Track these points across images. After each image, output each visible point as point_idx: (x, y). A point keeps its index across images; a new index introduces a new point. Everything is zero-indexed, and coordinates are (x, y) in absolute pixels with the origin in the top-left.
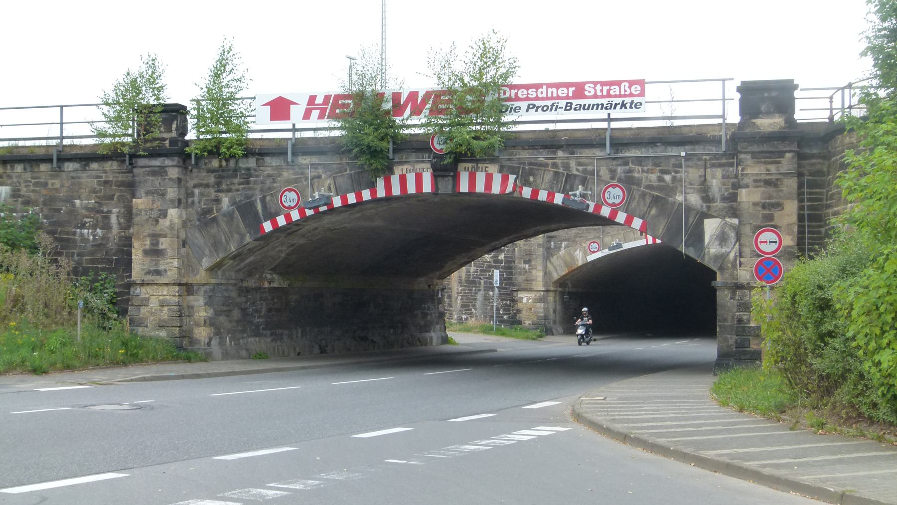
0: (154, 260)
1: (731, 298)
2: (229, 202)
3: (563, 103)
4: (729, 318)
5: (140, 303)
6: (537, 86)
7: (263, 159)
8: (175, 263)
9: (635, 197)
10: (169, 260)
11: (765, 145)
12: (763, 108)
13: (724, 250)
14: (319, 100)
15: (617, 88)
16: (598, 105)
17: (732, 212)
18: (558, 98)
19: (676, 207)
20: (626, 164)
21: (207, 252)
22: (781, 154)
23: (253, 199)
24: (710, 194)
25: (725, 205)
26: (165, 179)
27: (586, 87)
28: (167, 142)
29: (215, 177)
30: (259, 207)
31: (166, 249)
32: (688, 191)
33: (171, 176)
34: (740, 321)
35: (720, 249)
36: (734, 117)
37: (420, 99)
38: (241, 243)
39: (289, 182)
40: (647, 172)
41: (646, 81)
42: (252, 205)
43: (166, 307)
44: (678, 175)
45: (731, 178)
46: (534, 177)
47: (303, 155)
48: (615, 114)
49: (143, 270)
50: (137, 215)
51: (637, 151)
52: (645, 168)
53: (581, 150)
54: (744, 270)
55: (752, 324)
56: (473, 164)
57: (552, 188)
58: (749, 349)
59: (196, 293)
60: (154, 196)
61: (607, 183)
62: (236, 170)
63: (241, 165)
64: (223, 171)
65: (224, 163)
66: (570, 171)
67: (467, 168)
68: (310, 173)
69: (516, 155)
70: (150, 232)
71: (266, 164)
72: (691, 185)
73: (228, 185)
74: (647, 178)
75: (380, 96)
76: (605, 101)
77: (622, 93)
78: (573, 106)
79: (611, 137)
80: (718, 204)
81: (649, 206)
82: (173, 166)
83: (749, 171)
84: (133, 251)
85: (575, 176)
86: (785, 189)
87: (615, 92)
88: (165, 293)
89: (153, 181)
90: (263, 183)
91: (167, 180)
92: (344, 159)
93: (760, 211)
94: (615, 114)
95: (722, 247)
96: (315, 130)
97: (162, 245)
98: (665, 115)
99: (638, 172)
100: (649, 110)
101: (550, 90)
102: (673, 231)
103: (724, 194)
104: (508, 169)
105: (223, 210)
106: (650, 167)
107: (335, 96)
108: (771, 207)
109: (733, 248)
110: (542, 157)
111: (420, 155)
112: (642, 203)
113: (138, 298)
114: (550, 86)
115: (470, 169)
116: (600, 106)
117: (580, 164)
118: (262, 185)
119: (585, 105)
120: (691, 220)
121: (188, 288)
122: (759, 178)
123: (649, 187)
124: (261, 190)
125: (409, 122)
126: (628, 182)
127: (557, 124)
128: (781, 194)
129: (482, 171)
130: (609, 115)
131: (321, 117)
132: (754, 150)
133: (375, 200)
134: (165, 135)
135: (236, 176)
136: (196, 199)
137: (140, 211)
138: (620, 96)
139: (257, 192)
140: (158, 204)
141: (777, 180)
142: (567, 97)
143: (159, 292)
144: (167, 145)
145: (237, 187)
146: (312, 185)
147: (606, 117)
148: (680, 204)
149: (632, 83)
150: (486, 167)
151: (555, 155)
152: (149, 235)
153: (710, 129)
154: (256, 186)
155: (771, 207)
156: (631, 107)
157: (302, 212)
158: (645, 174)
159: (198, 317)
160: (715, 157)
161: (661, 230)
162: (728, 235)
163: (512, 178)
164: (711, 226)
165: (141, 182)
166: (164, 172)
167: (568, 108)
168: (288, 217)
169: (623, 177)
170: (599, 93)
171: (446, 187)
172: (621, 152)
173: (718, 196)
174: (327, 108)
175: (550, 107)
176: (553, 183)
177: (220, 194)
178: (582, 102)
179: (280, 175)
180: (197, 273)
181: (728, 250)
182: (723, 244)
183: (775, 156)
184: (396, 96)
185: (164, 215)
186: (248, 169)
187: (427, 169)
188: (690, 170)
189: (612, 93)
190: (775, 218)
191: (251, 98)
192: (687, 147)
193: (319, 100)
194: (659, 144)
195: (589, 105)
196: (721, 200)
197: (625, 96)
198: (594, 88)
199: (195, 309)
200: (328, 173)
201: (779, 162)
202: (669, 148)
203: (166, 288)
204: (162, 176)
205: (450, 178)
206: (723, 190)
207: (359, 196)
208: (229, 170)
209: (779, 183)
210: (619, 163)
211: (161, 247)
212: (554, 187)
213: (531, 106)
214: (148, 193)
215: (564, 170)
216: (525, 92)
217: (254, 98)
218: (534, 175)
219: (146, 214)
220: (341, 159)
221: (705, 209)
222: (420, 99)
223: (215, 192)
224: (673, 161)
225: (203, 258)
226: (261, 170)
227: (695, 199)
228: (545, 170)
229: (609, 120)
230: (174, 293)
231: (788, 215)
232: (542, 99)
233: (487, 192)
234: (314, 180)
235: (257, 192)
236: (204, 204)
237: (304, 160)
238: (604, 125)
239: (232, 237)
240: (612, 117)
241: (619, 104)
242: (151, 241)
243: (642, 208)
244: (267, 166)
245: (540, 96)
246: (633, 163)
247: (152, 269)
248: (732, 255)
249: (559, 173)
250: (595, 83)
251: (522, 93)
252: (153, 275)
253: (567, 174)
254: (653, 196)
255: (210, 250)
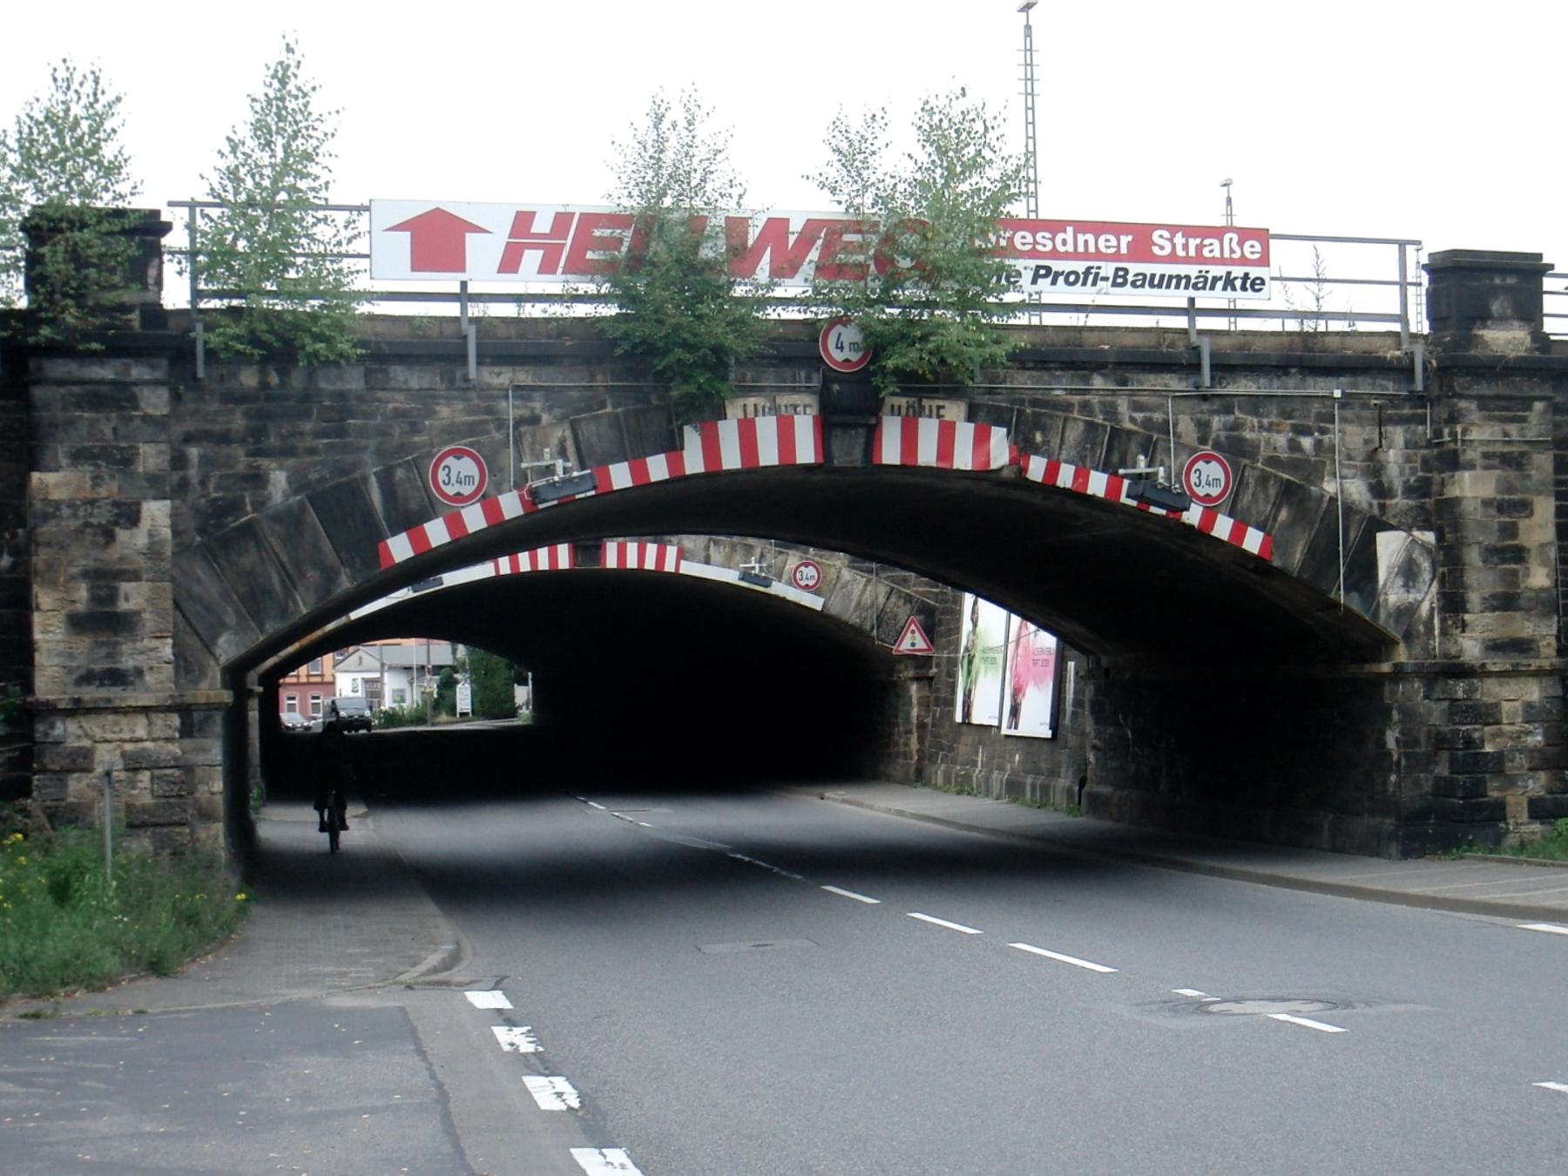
0: (103, 644)
1: (1426, 697)
2: (289, 482)
3: (1108, 269)
4: (1423, 738)
5: (65, 763)
6: (1056, 227)
7: (385, 370)
8: (167, 651)
9: (1248, 484)
10: (148, 643)
11: (1500, 383)
12: (1496, 307)
13: (1411, 597)
14: (542, 225)
15: (1216, 243)
16: (1179, 278)
17: (1422, 518)
18: (1099, 256)
19: (1325, 505)
20: (1228, 410)
21: (230, 619)
22: (1527, 403)
23: (357, 475)
24: (1384, 480)
25: (1411, 502)
26: (131, 419)
27: (1156, 236)
28: (135, 316)
29: (246, 415)
30: (376, 497)
31: (137, 613)
32: (1346, 472)
33: (150, 411)
34: (1469, 742)
35: (1405, 595)
36: (1420, 323)
37: (792, 239)
38: (328, 591)
39: (453, 432)
40: (1269, 430)
41: (1271, 232)
42: (356, 491)
43: (147, 773)
44: (1326, 438)
45: (1421, 447)
46: (1044, 435)
47: (493, 364)
48: (1204, 300)
49: (69, 670)
50: (46, 517)
51: (1251, 384)
52: (1265, 421)
53: (1141, 376)
54: (1471, 638)
55: (1489, 748)
56: (912, 400)
57: (1083, 459)
58: (1485, 799)
59: (201, 730)
60: (98, 466)
61: (1193, 450)
62: (306, 398)
63: (323, 385)
64: (269, 398)
65: (274, 379)
66: (1118, 422)
67: (896, 408)
68: (511, 410)
69: (1004, 381)
70: (89, 563)
71: (393, 384)
72: (1350, 458)
73: (283, 437)
74: (1268, 442)
75: (695, 224)
76: (1192, 271)
77: (1227, 255)
78: (1130, 278)
79: (1212, 355)
80: (1399, 502)
81: (1274, 504)
82: (156, 383)
83: (1474, 435)
84: (37, 618)
85: (1130, 433)
86: (1533, 472)
87: (1211, 251)
88: (141, 732)
89: (93, 423)
90: (383, 432)
91: (137, 422)
92: (599, 377)
93: (1493, 517)
94: (1204, 300)
95: (1408, 592)
96: (519, 299)
97: (127, 599)
98: (1293, 308)
99: (1252, 429)
100: (1274, 297)
101: (1081, 238)
102: (1322, 554)
103: (1408, 481)
104: (988, 413)
105: (271, 504)
106: (1274, 419)
107: (581, 214)
108: (1512, 507)
109: (1427, 593)
110: (1060, 387)
111: (787, 372)
112: (1262, 496)
113: (59, 749)
114: (1081, 227)
115: (903, 411)
116: (1184, 282)
117: (1138, 407)
118: (379, 439)
119: (1153, 276)
120: (1352, 535)
121: (190, 719)
122: (1491, 449)
123: (1273, 461)
124: (380, 453)
125: (779, 292)
126: (1234, 450)
127: (1091, 315)
128: (1529, 484)
129: (930, 416)
130: (1192, 301)
131: (547, 267)
132: (1481, 392)
133: (678, 480)
134: (130, 296)
135: (307, 415)
136: (193, 474)
137: (57, 505)
138: (1221, 261)
139: (367, 457)
140: (110, 488)
141: (1522, 454)
142: (1117, 257)
143: (121, 731)
144: (136, 324)
145: (309, 442)
146: (518, 441)
147: (1184, 304)
148: (1333, 500)
149: (1245, 234)
150: (939, 408)
151: (1088, 384)
152: (86, 574)
153: (1378, 342)
154: (364, 442)
155: (1512, 507)
156: (1244, 288)
157: (491, 508)
158: (1264, 434)
159: (207, 795)
160: (1392, 400)
161: (1298, 556)
162: (1419, 566)
163: (998, 435)
164: (1390, 547)
165: (54, 425)
166: (128, 400)
167: (1120, 280)
168: (455, 522)
169: (1223, 439)
170: (1181, 253)
171: (848, 453)
172: (1220, 383)
173: (1398, 485)
174: (564, 244)
175: (1082, 276)
176: (1084, 449)
177: (264, 462)
178: (1148, 269)
179: (430, 413)
180: (203, 674)
181: (1419, 597)
182: (1411, 584)
183: (1509, 408)
184: (736, 226)
185: (130, 516)
186: (342, 396)
187: (805, 406)
188: (1349, 428)
189: (1206, 252)
190: (1521, 532)
191: (350, 209)
192: (1342, 379)
193: (542, 225)
194: (1293, 370)
195: (1162, 276)
196: (1403, 493)
197: (1232, 262)
198: (1171, 240)
199: (199, 772)
200: (557, 411)
201: (1523, 420)
202: (1310, 381)
203: (141, 721)
204: (122, 408)
205: (862, 431)
206: (1407, 471)
207: (639, 471)
208: (287, 398)
209: (1524, 462)
210: (1215, 407)
211: (123, 606)
212: (1086, 456)
213: (1042, 272)
214: (78, 457)
215: (1104, 419)
216: (1030, 239)
217: (360, 209)
218: (1044, 430)
219: (75, 515)
220: (592, 378)
221: (1376, 511)
222: (792, 239)
223: (249, 455)
224: (1316, 407)
225: (217, 635)
226: (379, 400)
227: (1357, 490)
228: (1066, 420)
229: (1191, 310)
230: (169, 733)
231: (1541, 526)
232: (1066, 256)
233: (943, 465)
234: (523, 429)
235: (367, 457)
236: (218, 488)
237: (502, 377)
238: (1181, 322)
239: (302, 575)
240: (1198, 305)
241: (1221, 277)
242: (91, 589)
243: (1261, 505)
244: (394, 389)
245: (1061, 249)
246: (1241, 410)
247: (97, 667)
248: (1425, 609)
249: (1098, 424)
250: (1173, 229)
251: (1022, 240)
252: (102, 685)
253: (1112, 428)
254: (1282, 479)
255: (237, 612)
